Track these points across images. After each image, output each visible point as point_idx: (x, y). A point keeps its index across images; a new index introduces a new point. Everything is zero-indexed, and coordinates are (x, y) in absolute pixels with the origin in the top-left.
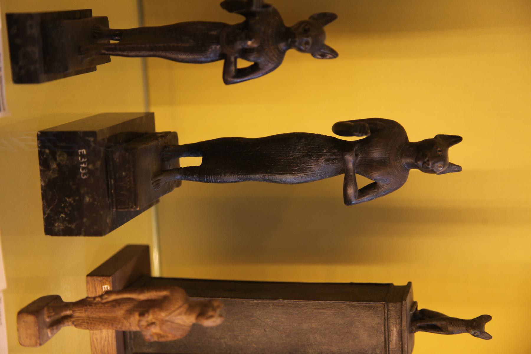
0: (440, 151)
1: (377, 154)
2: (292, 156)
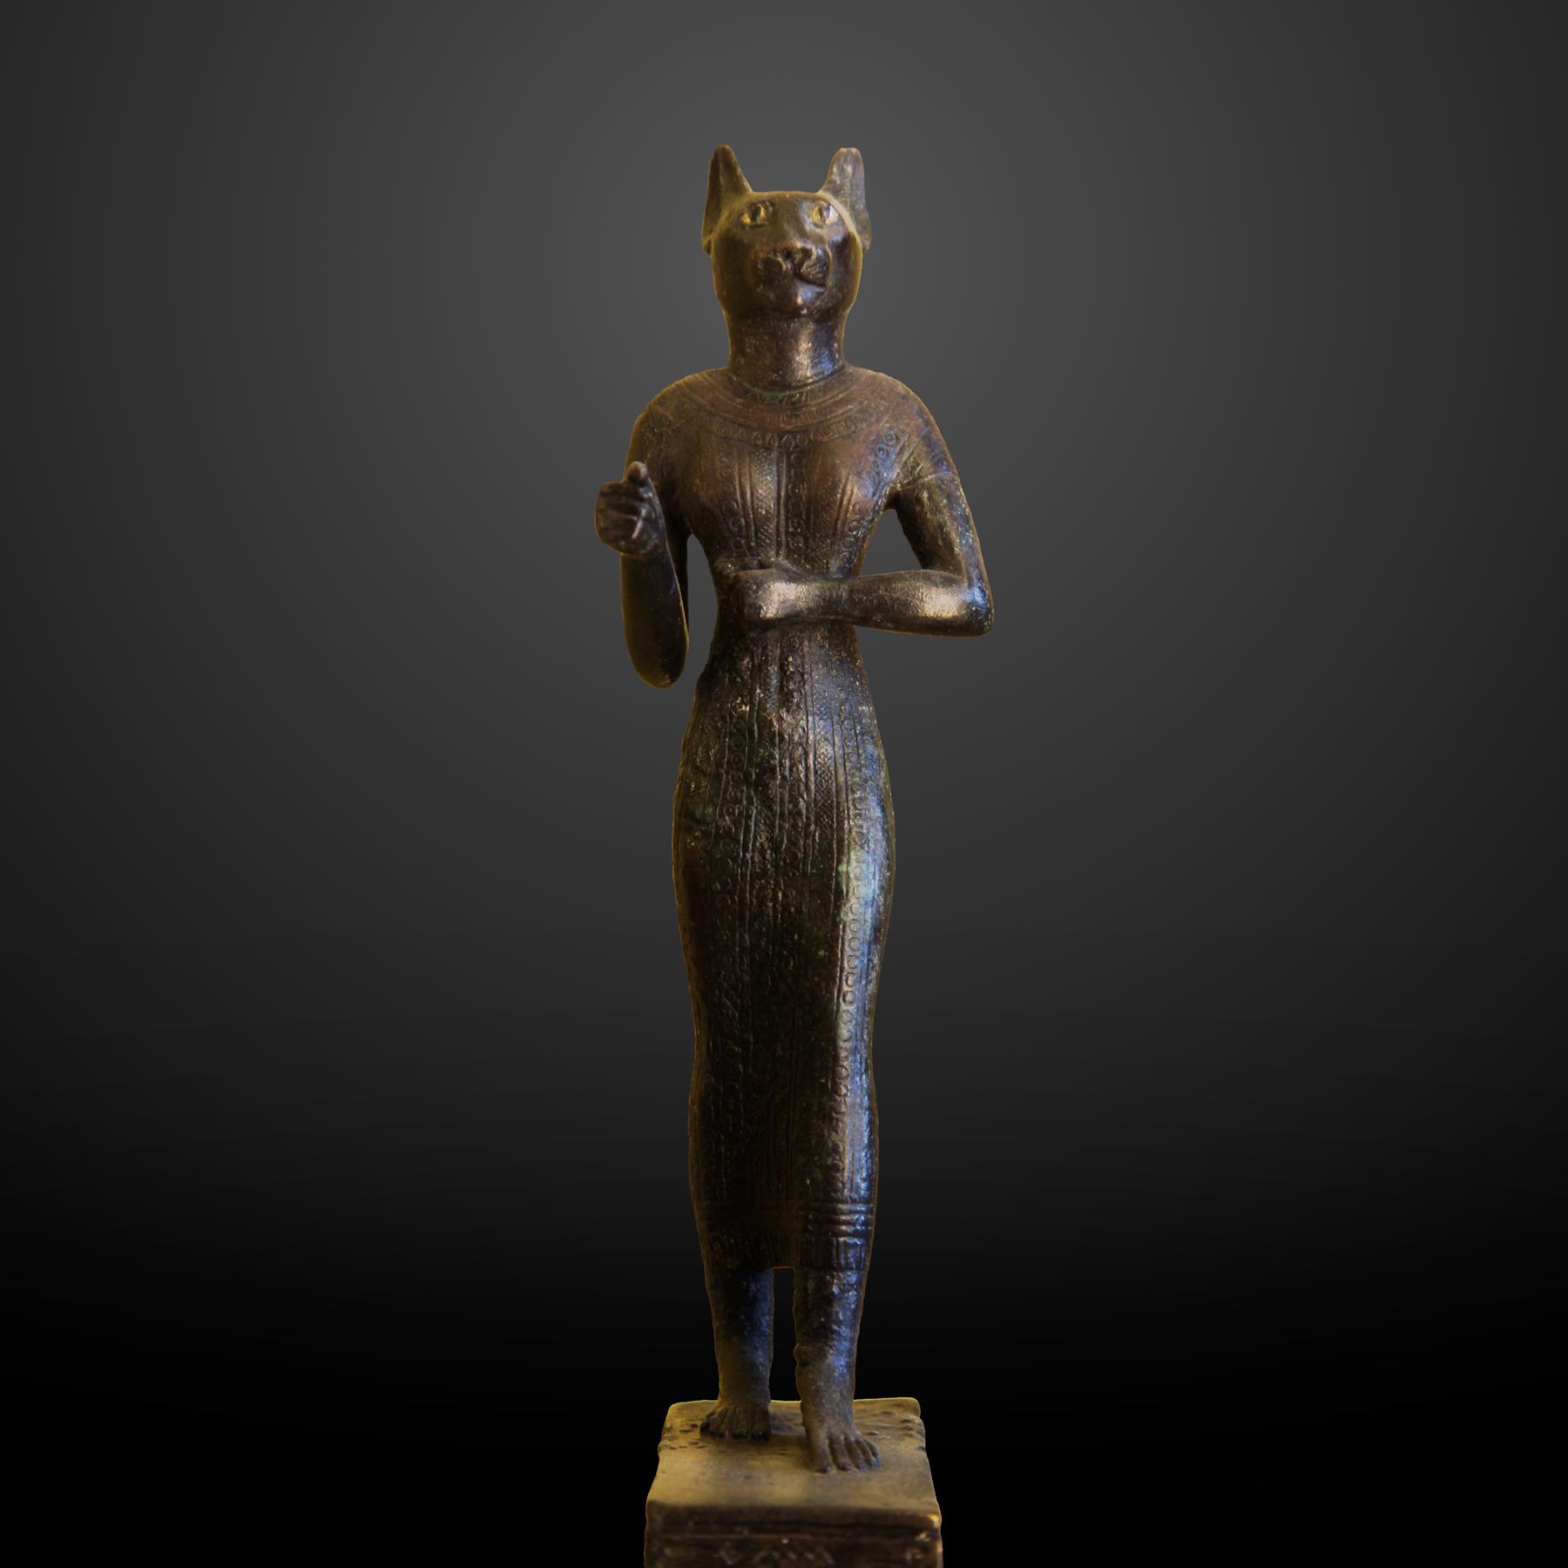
0: (754, 214)
1: (764, 487)
2: (762, 852)
